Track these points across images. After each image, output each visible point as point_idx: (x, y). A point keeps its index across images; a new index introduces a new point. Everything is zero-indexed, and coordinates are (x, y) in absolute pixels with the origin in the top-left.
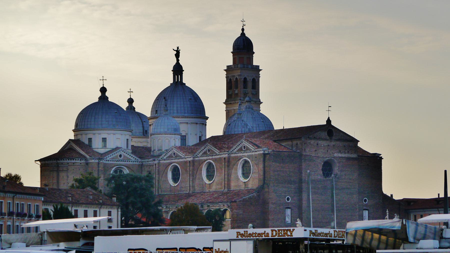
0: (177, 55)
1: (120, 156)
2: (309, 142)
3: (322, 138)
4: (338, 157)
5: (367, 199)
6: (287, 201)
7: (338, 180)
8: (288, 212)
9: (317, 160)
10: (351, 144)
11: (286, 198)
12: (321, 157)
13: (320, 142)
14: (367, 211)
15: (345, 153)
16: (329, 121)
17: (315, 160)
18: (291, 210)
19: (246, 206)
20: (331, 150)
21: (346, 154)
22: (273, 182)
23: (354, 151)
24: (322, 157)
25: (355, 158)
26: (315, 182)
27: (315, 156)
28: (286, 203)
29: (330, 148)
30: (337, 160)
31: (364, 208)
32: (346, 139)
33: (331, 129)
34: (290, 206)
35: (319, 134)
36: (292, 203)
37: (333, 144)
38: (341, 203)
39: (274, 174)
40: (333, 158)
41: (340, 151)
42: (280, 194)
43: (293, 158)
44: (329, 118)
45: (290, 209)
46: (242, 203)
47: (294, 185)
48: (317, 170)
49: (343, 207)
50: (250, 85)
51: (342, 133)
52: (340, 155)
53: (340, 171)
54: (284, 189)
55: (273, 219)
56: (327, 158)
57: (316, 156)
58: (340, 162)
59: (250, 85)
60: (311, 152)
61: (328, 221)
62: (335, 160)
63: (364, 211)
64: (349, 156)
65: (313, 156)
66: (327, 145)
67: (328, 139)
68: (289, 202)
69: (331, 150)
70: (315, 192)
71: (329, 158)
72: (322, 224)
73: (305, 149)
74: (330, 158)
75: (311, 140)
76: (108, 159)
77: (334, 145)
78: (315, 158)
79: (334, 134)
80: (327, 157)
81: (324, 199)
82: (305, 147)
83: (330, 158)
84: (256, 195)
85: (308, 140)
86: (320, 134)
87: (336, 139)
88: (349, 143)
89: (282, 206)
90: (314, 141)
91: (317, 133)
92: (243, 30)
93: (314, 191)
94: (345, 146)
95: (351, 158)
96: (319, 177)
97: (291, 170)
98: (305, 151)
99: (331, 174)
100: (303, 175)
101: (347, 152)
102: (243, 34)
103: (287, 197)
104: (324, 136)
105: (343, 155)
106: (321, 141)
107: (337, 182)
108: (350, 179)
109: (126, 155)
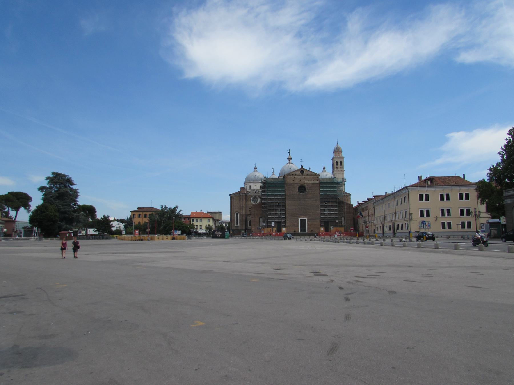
0: (289, 153)
1: (255, 192)
10: (315, 176)
13: (296, 176)
15: (312, 181)
16: (302, 166)
21: (312, 181)
25: (317, 183)
44: (302, 165)
50: (339, 164)
52: (308, 182)
59: (339, 164)
76: (249, 193)
92: (337, 143)
96: (296, 193)
102: (337, 145)
105: (310, 182)
109: (258, 192)
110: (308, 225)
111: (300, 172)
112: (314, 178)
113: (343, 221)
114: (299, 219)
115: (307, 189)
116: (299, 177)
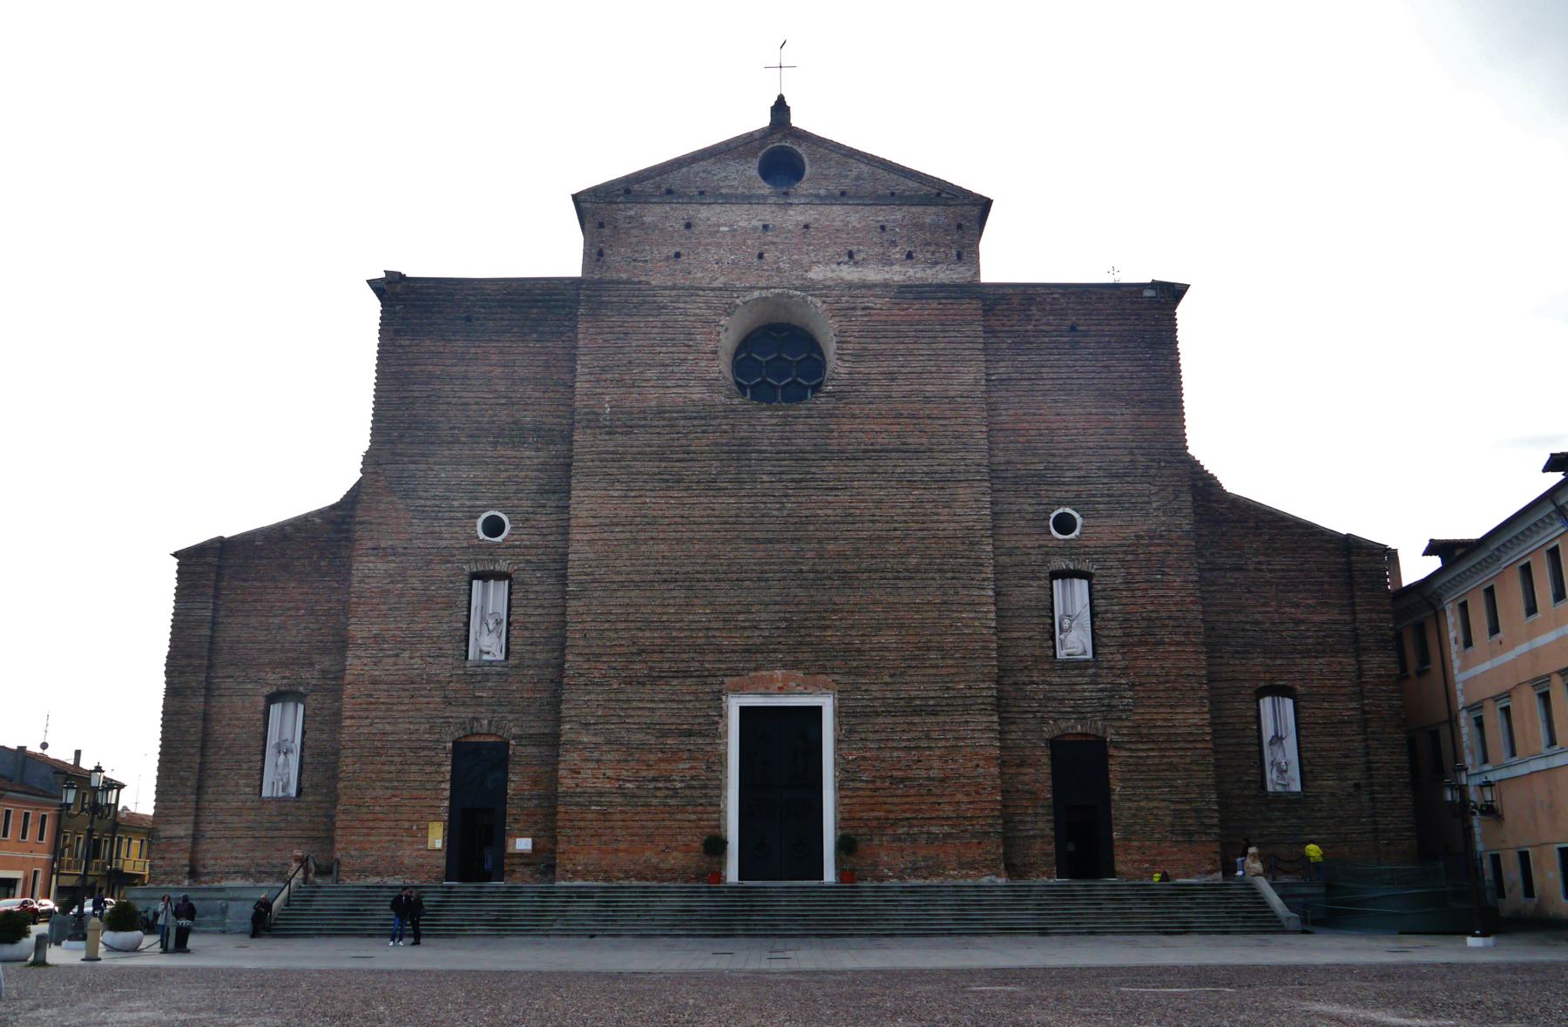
2: (632, 213)
3: (724, 191)
4: (837, 285)
5: (1076, 515)
6: (482, 535)
7: (834, 408)
8: (492, 599)
9: (686, 302)
11: (480, 522)
12: (713, 289)
14: (1085, 583)
15: (887, 261)
17: (664, 308)
18: (510, 587)
19: (245, 580)
20: (782, 252)
21: (896, 268)
22: (389, 435)
23: (954, 253)
24: (720, 289)
26: (664, 419)
27: (669, 284)
28: (473, 547)
29: (775, 240)
30: (824, 302)
31: (1060, 563)
32: (893, 194)
33: (787, 145)
34: (502, 566)
35: (704, 175)
36: (520, 547)
37: (801, 218)
38: (864, 534)
39: (405, 394)
40: (796, 289)
41: (851, 255)
42: (434, 498)
43: (535, 311)
44: (781, 99)
45: (504, 586)
46: (209, 559)
47: (538, 450)
48: (682, 356)
49: (873, 557)
51: (862, 166)
52: (849, 273)
53: (846, 358)
54: (466, 473)
55: (377, 638)
56: (756, 294)
57: (680, 281)
58: (854, 309)
60: (641, 264)
61: (761, 640)
62: (810, 298)
63: (1057, 584)
64: (918, 275)
65: (654, 283)
66: (755, 229)
67: (765, 197)
68: (498, 544)
69: (782, 252)
70: (666, 477)
71: (765, 293)
72: (710, 657)
73: (601, 253)
74: (779, 291)
75: (645, 203)
77: (806, 226)
78: (673, 293)
79: (808, 171)
80: (752, 288)
81: (733, 512)
82: (602, 242)
83: (777, 291)
84: (318, 520)
85: (621, 206)
86: (704, 171)
87: (822, 192)
88: (913, 209)
89: (448, 562)
90: (668, 209)
91: (684, 170)
93: (657, 470)
94: (889, 226)
95: (930, 285)
96: (697, 393)
97: (522, 372)
98: (598, 260)
99: (817, 389)
100: (581, 386)
101: (898, 256)
103: (484, 516)
104: (735, 183)
105: (873, 274)
106: (718, 208)
107: (831, 416)
108: (927, 400)
110: (840, 786)
111: (752, 170)
112: (920, 227)
113: (1278, 739)
114: (734, 705)
115: (831, 348)
116: (744, 218)
